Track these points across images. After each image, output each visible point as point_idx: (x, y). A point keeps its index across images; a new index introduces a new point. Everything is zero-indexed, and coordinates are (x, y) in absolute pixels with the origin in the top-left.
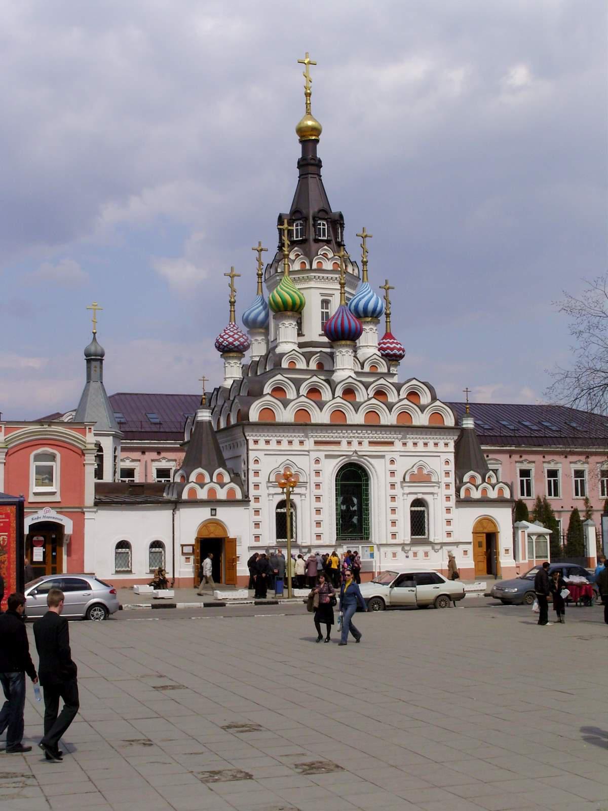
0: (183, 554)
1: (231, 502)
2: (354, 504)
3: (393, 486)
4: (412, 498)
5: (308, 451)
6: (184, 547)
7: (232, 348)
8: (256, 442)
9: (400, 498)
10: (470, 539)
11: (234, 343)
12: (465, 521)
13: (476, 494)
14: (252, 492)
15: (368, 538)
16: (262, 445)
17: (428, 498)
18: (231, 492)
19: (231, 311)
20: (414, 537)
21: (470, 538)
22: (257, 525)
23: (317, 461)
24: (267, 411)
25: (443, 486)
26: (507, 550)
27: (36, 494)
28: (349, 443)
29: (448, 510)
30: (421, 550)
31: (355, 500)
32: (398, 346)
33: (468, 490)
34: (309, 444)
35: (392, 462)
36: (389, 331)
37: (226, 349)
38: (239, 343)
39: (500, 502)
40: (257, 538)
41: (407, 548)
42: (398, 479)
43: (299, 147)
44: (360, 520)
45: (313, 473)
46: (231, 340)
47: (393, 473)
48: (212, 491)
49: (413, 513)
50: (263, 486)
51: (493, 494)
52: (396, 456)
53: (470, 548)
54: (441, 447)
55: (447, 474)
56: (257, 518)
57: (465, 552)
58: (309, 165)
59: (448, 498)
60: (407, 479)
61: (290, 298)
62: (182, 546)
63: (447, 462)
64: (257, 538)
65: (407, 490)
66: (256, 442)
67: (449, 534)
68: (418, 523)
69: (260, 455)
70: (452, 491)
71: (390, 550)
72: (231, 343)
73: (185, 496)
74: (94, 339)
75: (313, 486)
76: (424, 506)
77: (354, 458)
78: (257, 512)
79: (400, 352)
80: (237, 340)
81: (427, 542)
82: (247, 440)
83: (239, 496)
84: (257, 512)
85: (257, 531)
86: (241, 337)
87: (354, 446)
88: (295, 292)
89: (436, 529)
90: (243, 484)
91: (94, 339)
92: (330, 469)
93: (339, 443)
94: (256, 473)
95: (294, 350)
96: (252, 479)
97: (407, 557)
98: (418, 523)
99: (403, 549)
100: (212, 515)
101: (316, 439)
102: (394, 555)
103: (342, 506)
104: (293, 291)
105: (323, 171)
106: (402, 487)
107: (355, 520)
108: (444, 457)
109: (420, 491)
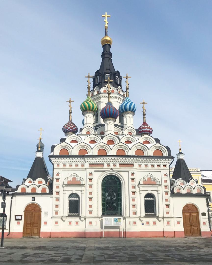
0: (16, 219)
1: (43, 193)
2: (115, 196)
3: (133, 187)
4: (146, 193)
5: (85, 169)
6: (16, 216)
7: (67, 130)
8: (58, 165)
9: (138, 193)
10: (182, 216)
11: (68, 128)
12: (178, 205)
14: (55, 189)
15: (121, 214)
16: (61, 166)
17: (155, 193)
18: (44, 189)
19: (69, 116)
20: (146, 214)
21: (181, 215)
22: (57, 206)
25: (163, 187)
26: (204, 223)
28: (109, 165)
29: (167, 200)
30: (151, 220)
31: (115, 194)
32: (151, 128)
33: (179, 189)
34: (87, 165)
35: (133, 174)
36: (145, 122)
37: (65, 131)
38: (70, 128)
39: (199, 195)
40: (57, 213)
41: (142, 219)
42: (136, 183)
44: (117, 204)
45: (88, 180)
46: (66, 127)
47: (133, 180)
48: (34, 189)
49: (146, 202)
52: (135, 171)
53: (181, 220)
54: (162, 167)
55: (166, 181)
56: (57, 203)
57: (178, 223)
59: (166, 193)
60: (141, 183)
61: (87, 105)
62: (16, 216)
63: (165, 175)
64: (57, 213)
66: (58, 165)
67: (168, 213)
68: (150, 206)
69: (60, 171)
70: (169, 190)
71: (132, 220)
72: (67, 128)
73: (19, 191)
75: (88, 186)
76: (153, 198)
77: (111, 173)
78: (57, 199)
79: (149, 129)
80: (69, 126)
81: (155, 216)
82: (53, 164)
83: (48, 191)
84: (57, 199)
85: (57, 209)
86: (71, 125)
87: (112, 166)
88: (90, 102)
89: (160, 210)
90: (51, 186)
92: (98, 179)
94: (58, 180)
95: (88, 126)
96: (55, 183)
97: (143, 224)
98: (150, 206)
99: (140, 219)
100: (32, 201)
101: (90, 163)
102: (135, 223)
103: (108, 197)
104: (89, 101)
106: (139, 187)
107: (115, 204)
108: (163, 172)
109: (150, 189)
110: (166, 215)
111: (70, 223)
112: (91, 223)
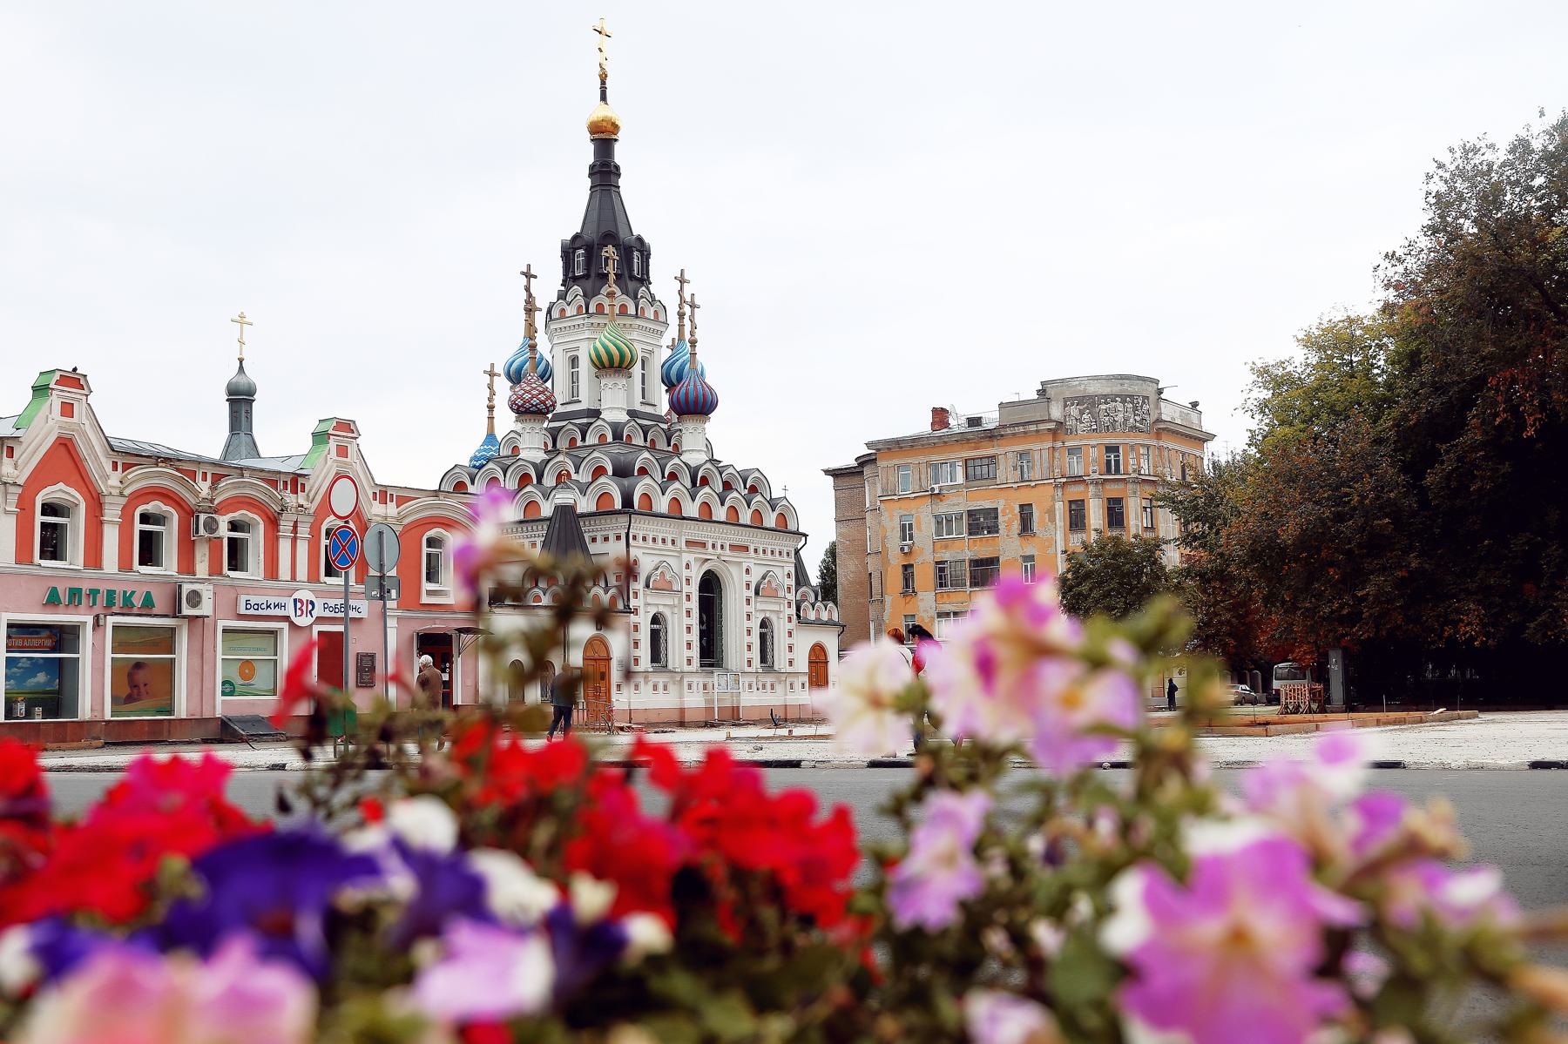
13: (812, 616)
23: (688, 566)
24: (646, 497)
27: (429, 593)
29: (790, 634)
35: (747, 571)
39: (829, 623)
43: (591, 147)
50: (641, 594)
51: (825, 616)
53: (806, 679)
58: (604, 174)
65: (759, 606)
66: (635, 538)
70: (793, 611)
72: (543, 402)
74: (241, 367)
91: (241, 367)
93: (704, 545)
105: (621, 182)
110: (790, 669)
111: (655, 688)
112: (690, 686)
